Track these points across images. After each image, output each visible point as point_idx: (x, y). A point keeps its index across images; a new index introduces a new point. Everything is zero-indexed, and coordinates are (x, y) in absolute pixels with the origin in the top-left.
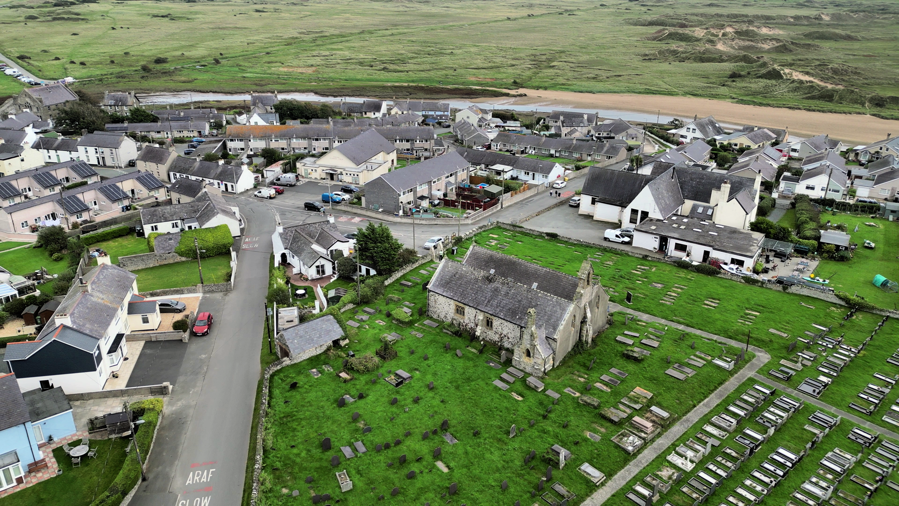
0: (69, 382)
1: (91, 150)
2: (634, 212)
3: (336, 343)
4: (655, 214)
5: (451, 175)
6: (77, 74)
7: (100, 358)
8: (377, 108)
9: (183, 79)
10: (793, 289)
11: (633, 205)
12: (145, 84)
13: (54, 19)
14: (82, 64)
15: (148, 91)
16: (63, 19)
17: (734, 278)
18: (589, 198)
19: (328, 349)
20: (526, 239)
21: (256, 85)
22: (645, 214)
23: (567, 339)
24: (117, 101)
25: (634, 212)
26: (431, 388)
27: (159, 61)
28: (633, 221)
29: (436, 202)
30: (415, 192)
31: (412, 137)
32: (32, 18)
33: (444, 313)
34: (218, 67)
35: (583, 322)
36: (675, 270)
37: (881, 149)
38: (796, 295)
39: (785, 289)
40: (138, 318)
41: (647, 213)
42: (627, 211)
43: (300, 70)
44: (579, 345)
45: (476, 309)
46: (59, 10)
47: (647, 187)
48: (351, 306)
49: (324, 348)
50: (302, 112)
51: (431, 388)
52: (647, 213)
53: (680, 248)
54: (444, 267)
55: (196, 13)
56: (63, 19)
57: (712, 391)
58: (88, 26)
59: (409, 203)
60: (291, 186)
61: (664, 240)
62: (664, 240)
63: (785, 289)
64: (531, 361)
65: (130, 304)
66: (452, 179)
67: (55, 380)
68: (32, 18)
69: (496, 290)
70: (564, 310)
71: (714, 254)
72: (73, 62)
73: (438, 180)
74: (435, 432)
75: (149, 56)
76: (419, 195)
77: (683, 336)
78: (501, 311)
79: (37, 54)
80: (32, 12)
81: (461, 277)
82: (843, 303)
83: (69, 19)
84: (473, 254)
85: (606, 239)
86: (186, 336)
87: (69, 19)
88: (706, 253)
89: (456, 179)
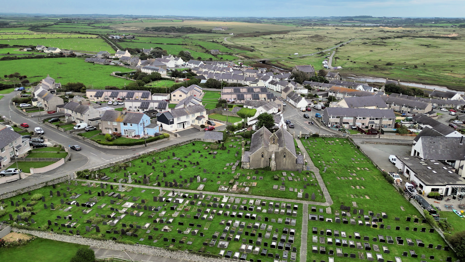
0: (165, 126)
1: (280, 86)
3: (219, 141)
4: (421, 156)
5: (377, 119)
6: (346, 66)
7: (172, 123)
8: (452, 95)
9: (387, 72)
12: (369, 73)
13: (373, 45)
14: (355, 62)
15: (363, 76)
16: (377, 44)
19: (216, 142)
21: (419, 79)
22: (418, 153)
23: (259, 161)
24: (331, 75)
26: (214, 157)
27: (389, 64)
29: (354, 127)
30: (341, 119)
31: (413, 106)
32: (365, 43)
34: (415, 70)
35: (270, 159)
40: (197, 121)
43: (456, 76)
44: (267, 169)
46: (379, 40)
47: (420, 138)
48: (241, 137)
49: (215, 141)
50: (398, 90)
51: (214, 157)
53: (408, 172)
55: (447, 45)
56: (377, 44)
57: (278, 197)
58: (385, 48)
59: (336, 123)
60: (318, 110)
65: (198, 117)
66: (377, 122)
67: (163, 124)
68: (365, 43)
72: (352, 61)
73: (364, 118)
74: (194, 164)
75: (385, 62)
76: (344, 121)
77: (315, 185)
79: (345, 57)
80: (367, 41)
83: (379, 45)
86: (201, 129)
87: (379, 45)
89: (381, 122)
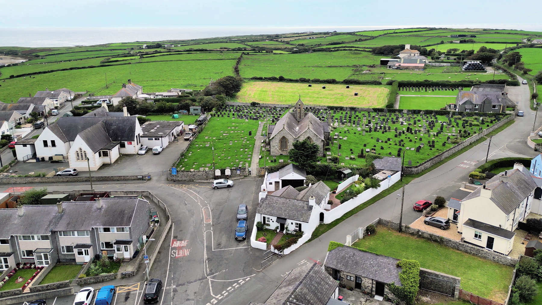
18: (97, 154)
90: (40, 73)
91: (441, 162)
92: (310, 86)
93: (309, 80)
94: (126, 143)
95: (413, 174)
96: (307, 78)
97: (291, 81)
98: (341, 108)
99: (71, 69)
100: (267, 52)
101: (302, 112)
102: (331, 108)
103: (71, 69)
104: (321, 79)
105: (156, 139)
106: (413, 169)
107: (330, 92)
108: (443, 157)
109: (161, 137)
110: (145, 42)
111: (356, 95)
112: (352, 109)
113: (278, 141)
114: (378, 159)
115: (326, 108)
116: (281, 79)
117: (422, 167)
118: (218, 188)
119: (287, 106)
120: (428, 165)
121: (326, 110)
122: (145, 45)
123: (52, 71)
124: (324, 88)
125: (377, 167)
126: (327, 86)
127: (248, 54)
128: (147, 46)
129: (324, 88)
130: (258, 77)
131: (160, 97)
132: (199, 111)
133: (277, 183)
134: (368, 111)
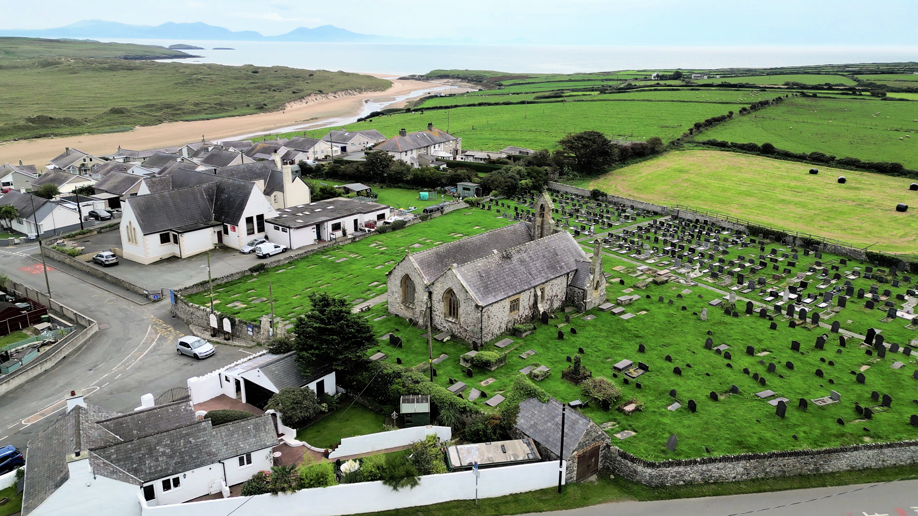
2: (249, 220)
10: (447, 210)
11: (246, 214)
17: (415, 222)
18: (157, 237)
20: (243, 286)
22: (260, 218)
25: (249, 220)
28: (250, 232)
33: (498, 325)
36: (388, 235)
37: (85, 160)
38: (451, 212)
39: (442, 212)
41: (262, 215)
42: (242, 222)
45: (529, 289)
52: (262, 215)
53: (336, 227)
54: (464, 276)
61: (319, 227)
62: (319, 227)
63: (442, 212)
64: (599, 289)
69: (521, 261)
70: (568, 240)
71: (364, 219)
78: (545, 273)
81: (488, 273)
82: (468, 205)
84: (421, 262)
85: (264, 257)
88: (356, 221)
90: (441, 108)
91: (817, 479)
92: (813, 172)
93: (833, 158)
94: (229, 226)
95: (638, 483)
96: (828, 155)
97: (786, 156)
98: (779, 237)
99: (480, 104)
100: (873, 95)
101: (546, 226)
102: (754, 231)
103: (480, 104)
104: (864, 158)
105: (283, 230)
106: (640, 468)
107: (851, 194)
108: (842, 463)
109: (289, 228)
110: (654, 71)
111: (901, 209)
112: (809, 244)
113: (398, 282)
114: (534, 401)
115: (742, 228)
116: (767, 151)
117: (692, 473)
118: (182, 354)
119: (658, 210)
120: (734, 471)
121: (739, 233)
122: (655, 74)
123: (456, 106)
124: (842, 181)
125: (521, 422)
126: (850, 175)
127: (815, 96)
128: (658, 76)
129: (842, 181)
130: (720, 140)
131: (470, 160)
132: (472, 192)
133: (238, 383)
134: (847, 256)
